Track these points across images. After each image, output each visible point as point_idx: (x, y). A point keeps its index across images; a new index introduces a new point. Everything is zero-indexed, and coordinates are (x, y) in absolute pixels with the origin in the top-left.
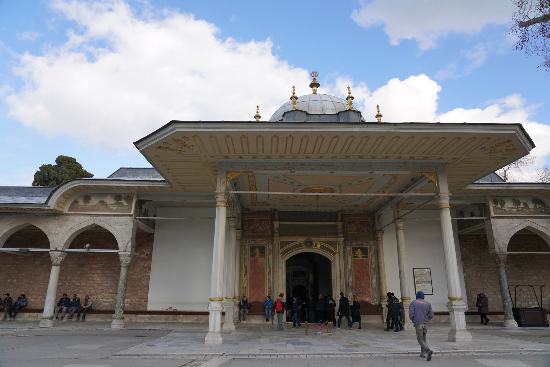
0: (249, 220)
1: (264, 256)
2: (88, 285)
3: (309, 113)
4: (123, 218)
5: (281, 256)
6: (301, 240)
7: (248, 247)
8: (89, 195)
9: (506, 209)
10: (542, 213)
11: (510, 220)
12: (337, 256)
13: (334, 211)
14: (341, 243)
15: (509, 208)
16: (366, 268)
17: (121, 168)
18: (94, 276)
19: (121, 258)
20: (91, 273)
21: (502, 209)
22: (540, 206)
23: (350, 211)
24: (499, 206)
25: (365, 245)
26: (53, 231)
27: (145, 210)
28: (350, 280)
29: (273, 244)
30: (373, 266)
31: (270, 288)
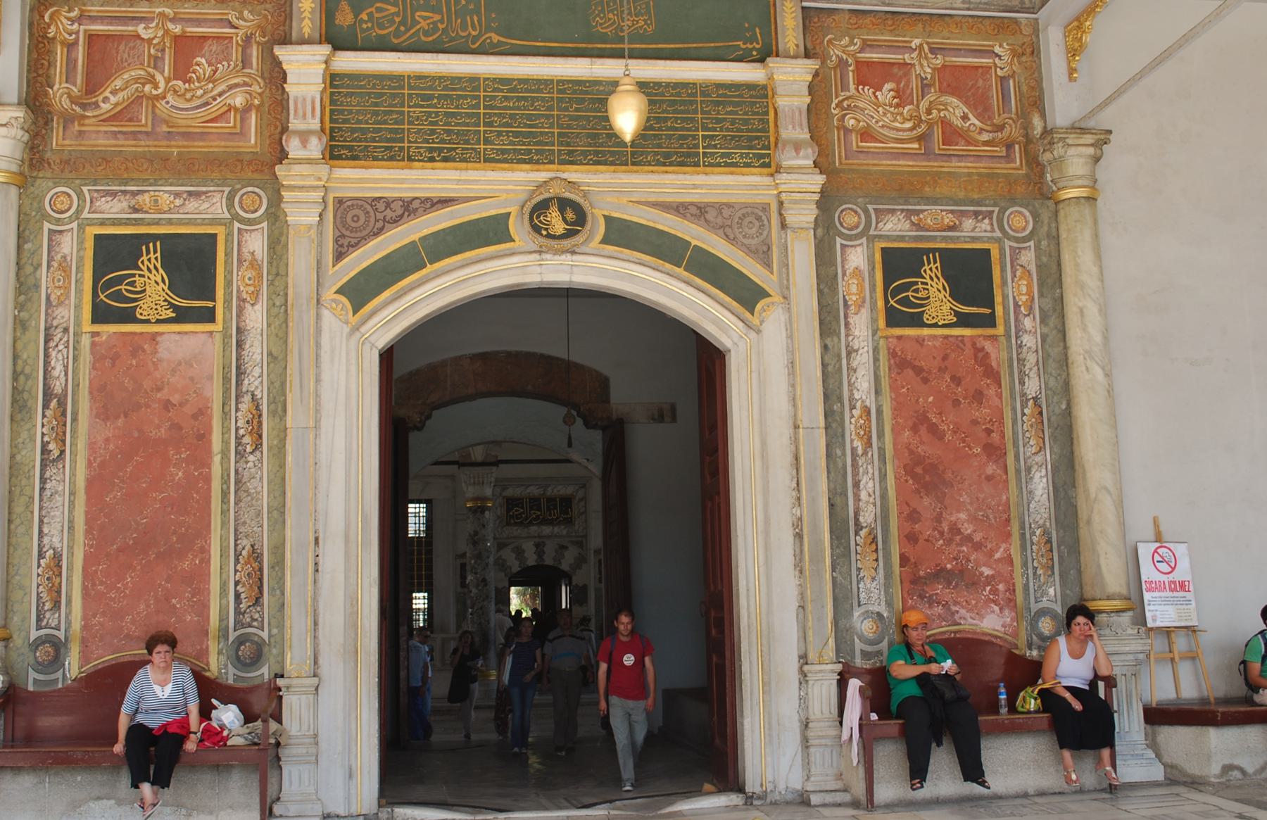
0: (92, 38)
1: (208, 316)
5: (335, 319)
7: (75, 248)
12: (772, 318)
14: (803, 215)
16: (979, 397)
25: (974, 232)
28: (869, 485)
29: (275, 215)
30: (1032, 386)
31: (256, 555)
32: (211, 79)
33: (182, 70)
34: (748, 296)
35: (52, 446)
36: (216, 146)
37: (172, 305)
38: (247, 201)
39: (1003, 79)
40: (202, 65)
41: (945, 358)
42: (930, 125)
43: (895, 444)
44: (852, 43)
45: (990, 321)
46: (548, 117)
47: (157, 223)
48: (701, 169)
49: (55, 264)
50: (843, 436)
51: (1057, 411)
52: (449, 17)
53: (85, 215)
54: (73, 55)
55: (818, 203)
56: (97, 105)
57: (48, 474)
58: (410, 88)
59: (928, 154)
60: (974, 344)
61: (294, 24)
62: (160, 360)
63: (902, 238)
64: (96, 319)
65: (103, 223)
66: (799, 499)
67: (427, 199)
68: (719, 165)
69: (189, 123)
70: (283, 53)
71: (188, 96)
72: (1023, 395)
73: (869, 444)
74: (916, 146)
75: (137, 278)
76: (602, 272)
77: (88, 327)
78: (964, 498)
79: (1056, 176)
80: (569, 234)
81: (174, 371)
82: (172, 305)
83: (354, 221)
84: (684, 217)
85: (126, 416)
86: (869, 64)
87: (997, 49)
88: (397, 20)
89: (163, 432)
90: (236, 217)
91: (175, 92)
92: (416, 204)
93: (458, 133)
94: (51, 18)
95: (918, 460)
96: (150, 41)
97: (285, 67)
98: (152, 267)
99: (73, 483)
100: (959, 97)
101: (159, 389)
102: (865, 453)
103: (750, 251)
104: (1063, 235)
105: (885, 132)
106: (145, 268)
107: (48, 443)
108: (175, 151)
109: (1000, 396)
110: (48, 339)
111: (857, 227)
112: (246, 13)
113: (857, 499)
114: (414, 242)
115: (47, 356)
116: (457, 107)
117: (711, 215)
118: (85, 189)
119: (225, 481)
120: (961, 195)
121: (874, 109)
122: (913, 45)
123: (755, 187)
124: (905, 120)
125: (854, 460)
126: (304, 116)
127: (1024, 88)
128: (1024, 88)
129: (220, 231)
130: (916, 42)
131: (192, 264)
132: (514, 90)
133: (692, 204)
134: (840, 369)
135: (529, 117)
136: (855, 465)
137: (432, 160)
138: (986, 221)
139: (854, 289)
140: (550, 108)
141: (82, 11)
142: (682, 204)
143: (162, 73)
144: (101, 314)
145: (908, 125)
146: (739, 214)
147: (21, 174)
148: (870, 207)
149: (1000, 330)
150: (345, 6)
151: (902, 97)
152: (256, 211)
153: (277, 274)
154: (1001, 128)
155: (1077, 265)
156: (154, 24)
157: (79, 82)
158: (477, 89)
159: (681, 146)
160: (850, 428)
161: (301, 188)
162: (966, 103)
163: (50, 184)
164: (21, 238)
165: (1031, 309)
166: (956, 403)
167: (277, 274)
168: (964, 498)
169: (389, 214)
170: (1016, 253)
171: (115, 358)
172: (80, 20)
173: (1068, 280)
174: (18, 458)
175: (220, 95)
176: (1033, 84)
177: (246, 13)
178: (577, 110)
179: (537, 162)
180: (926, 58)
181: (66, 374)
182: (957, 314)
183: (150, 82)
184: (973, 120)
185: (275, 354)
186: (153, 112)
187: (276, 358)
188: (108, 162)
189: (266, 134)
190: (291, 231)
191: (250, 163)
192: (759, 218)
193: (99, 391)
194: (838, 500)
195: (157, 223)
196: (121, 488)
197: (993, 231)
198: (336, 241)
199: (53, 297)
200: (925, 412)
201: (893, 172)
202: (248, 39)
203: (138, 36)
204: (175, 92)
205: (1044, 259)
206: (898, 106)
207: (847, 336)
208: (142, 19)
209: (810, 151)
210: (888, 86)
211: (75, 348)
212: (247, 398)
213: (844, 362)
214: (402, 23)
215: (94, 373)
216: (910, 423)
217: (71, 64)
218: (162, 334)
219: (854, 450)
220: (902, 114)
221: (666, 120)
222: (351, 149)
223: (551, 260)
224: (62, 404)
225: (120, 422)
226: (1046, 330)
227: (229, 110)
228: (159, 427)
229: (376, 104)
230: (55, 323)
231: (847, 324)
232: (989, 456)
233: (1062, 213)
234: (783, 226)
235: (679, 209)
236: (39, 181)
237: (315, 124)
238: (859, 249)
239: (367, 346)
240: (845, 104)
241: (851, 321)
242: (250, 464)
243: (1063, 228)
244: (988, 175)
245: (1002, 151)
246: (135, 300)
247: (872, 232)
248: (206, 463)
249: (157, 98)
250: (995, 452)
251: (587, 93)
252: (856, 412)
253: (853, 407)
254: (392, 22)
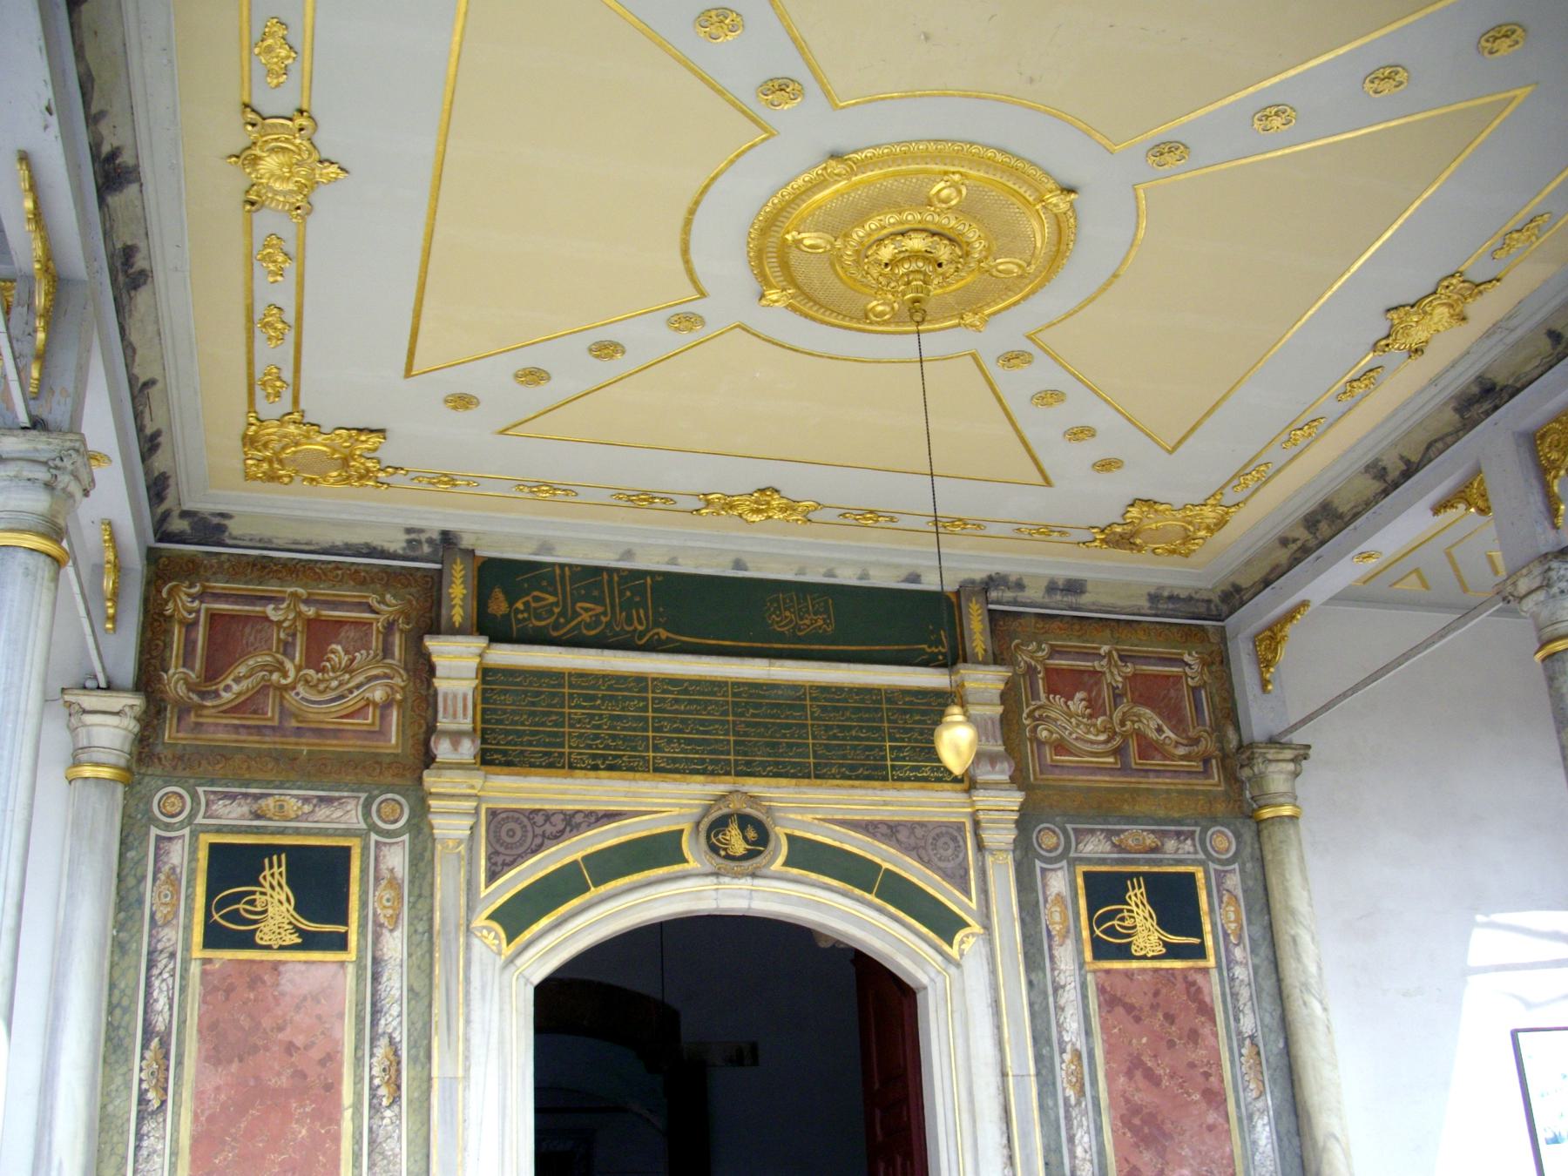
0: (213, 617)
1: (340, 943)
6: (669, 801)
7: (187, 858)
13: (930, 583)
14: (1001, 836)
16: (1194, 1036)
23: (1052, 588)
25: (1178, 856)
28: (1084, 1139)
29: (420, 826)
30: (1248, 1024)
32: (348, 669)
33: (315, 658)
34: (944, 924)
35: (151, 1095)
36: (351, 745)
37: (298, 930)
38: (386, 809)
39: (1195, 690)
40: (337, 653)
41: (1156, 994)
42: (1125, 737)
43: (1110, 1093)
44: (1040, 649)
45: (1199, 952)
46: (723, 723)
47: (282, 832)
48: (890, 783)
49: (162, 877)
50: (1054, 1084)
51: (1275, 1050)
52: (613, 612)
53: (200, 820)
54: (193, 636)
55: (1017, 822)
56: (217, 694)
57: (145, 1129)
58: (571, 686)
59: (1125, 769)
60: (1185, 978)
61: (444, 611)
62: (283, 994)
63: (1103, 861)
65: (219, 830)
66: (1011, 1158)
67: (592, 812)
68: (908, 779)
69: (321, 717)
70: (433, 644)
71: (322, 687)
72: (1240, 1033)
73: (1081, 1093)
74: (1111, 760)
75: (257, 896)
76: (786, 899)
77: (198, 952)
78: (1186, 1152)
79: (1256, 793)
80: (750, 855)
81: (298, 1008)
82: (298, 930)
83: (511, 835)
84: (874, 836)
85: (241, 1060)
86: (1058, 671)
87: (1187, 658)
88: (557, 610)
89: (284, 1082)
90: (373, 828)
91: (307, 682)
92: (579, 818)
93: (625, 739)
94: (169, 593)
95: (1135, 1110)
96: (279, 624)
97: (434, 659)
98: (275, 883)
99: (175, 1141)
100: (1153, 709)
101: (281, 1029)
102: (1078, 1103)
103: (947, 875)
104: (1269, 857)
105: (1078, 744)
106: (267, 885)
107: (147, 1091)
108: (305, 749)
109: (1216, 1035)
110: (151, 965)
111: (1056, 848)
112: (388, 596)
113: (1073, 1156)
114: (575, 862)
115: (149, 985)
116: (623, 709)
117: (903, 835)
118: (200, 790)
119: (357, 1141)
120: (1161, 813)
121: (1066, 719)
122: (1102, 652)
123: (950, 805)
124: (1099, 732)
125: (1067, 1112)
126: (455, 715)
127: (1217, 699)
128: (1217, 699)
129: (355, 844)
130: (1105, 649)
131: (321, 882)
132: (686, 692)
133: (882, 822)
134: (1047, 1008)
135: (702, 722)
136: (1068, 1118)
137: (595, 768)
138: (1189, 842)
139: (1057, 917)
140: (725, 713)
141: (204, 587)
142: (871, 822)
143: (292, 659)
144: (215, 937)
145: (1102, 737)
146: (933, 834)
147: (128, 769)
148: (1069, 827)
149: (1211, 962)
150: (498, 594)
151: (1094, 707)
152: (396, 821)
153: (420, 896)
154: (1195, 741)
155: (1286, 889)
156: (284, 606)
157: (198, 666)
158: (645, 689)
159: (868, 758)
160: (1061, 1075)
161: (452, 796)
162: (1160, 714)
163: (160, 782)
164: (124, 844)
165: (1240, 938)
166: (1171, 1044)
167: (420, 896)
168: (1186, 1152)
169: (549, 829)
170: (1221, 876)
171: (229, 990)
172: (201, 597)
173: (1277, 906)
174: (110, 1108)
175: (358, 687)
176: (1225, 695)
177: (388, 596)
178: (753, 715)
179: (712, 773)
180: (1116, 666)
181: (171, 1008)
182: (1166, 944)
183: (278, 670)
184: (1168, 733)
185: (417, 987)
186: (281, 705)
187: (417, 994)
188: (227, 759)
189: (409, 733)
190: (439, 847)
191: (390, 765)
192: (954, 839)
193: (210, 1029)
194: (1053, 1159)
195: (282, 832)
196: (233, 1148)
197: (1196, 852)
198: (489, 858)
199: (158, 916)
200: (1138, 1057)
201: (1090, 789)
202: (390, 627)
203: (267, 618)
204: (307, 682)
205: (1250, 883)
206: (1090, 716)
207: (1053, 970)
208: (270, 599)
209: (1006, 765)
210: (1079, 695)
211: (182, 977)
212: (384, 1042)
213: (1051, 999)
214: (563, 614)
215: (204, 1007)
216: (1124, 1068)
217: (189, 646)
218: (284, 963)
219: (1066, 1100)
220: (1095, 725)
221: (850, 728)
222: (505, 753)
223: (728, 883)
224: (164, 1044)
225: (234, 1067)
226: (1257, 961)
227: (367, 705)
228: (279, 1074)
229: (533, 704)
230: (160, 946)
231: (1052, 957)
232: (1209, 1102)
233: (1265, 833)
234: (980, 847)
235: (868, 828)
236: (147, 779)
237: (467, 724)
238: (1060, 873)
239: (522, 981)
240: (1037, 714)
241: (1056, 953)
242: (387, 1121)
243: (1267, 848)
244: (1187, 792)
245: (1197, 765)
246: (255, 922)
247: (1072, 855)
248: (334, 1119)
249: (286, 688)
250: (1215, 1098)
251: (764, 697)
252: (1067, 1057)
253: (1063, 1051)
254: (551, 612)
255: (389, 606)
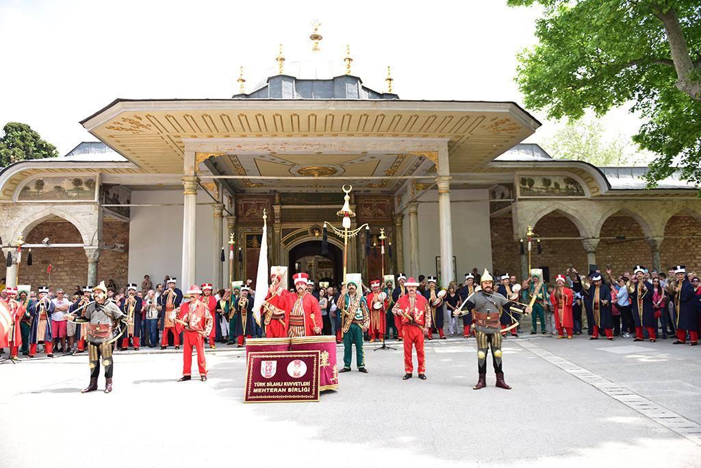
2: (55, 284)
3: (297, 78)
4: (85, 206)
6: (306, 226)
7: (243, 237)
8: (41, 179)
9: (534, 190)
10: (573, 194)
11: (538, 203)
15: (538, 188)
17: (83, 142)
18: (61, 274)
19: (87, 253)
20: (57, 271)
21: (530, 190)
22: (572, 186)
23: (365, 191)
24: (527, 186)
26: (4, 225)
27: (114, 195)
64: (247, 247)
255: (268, 201)
